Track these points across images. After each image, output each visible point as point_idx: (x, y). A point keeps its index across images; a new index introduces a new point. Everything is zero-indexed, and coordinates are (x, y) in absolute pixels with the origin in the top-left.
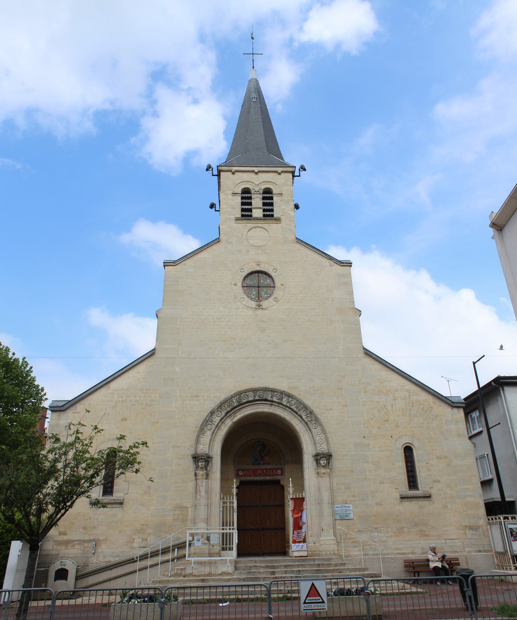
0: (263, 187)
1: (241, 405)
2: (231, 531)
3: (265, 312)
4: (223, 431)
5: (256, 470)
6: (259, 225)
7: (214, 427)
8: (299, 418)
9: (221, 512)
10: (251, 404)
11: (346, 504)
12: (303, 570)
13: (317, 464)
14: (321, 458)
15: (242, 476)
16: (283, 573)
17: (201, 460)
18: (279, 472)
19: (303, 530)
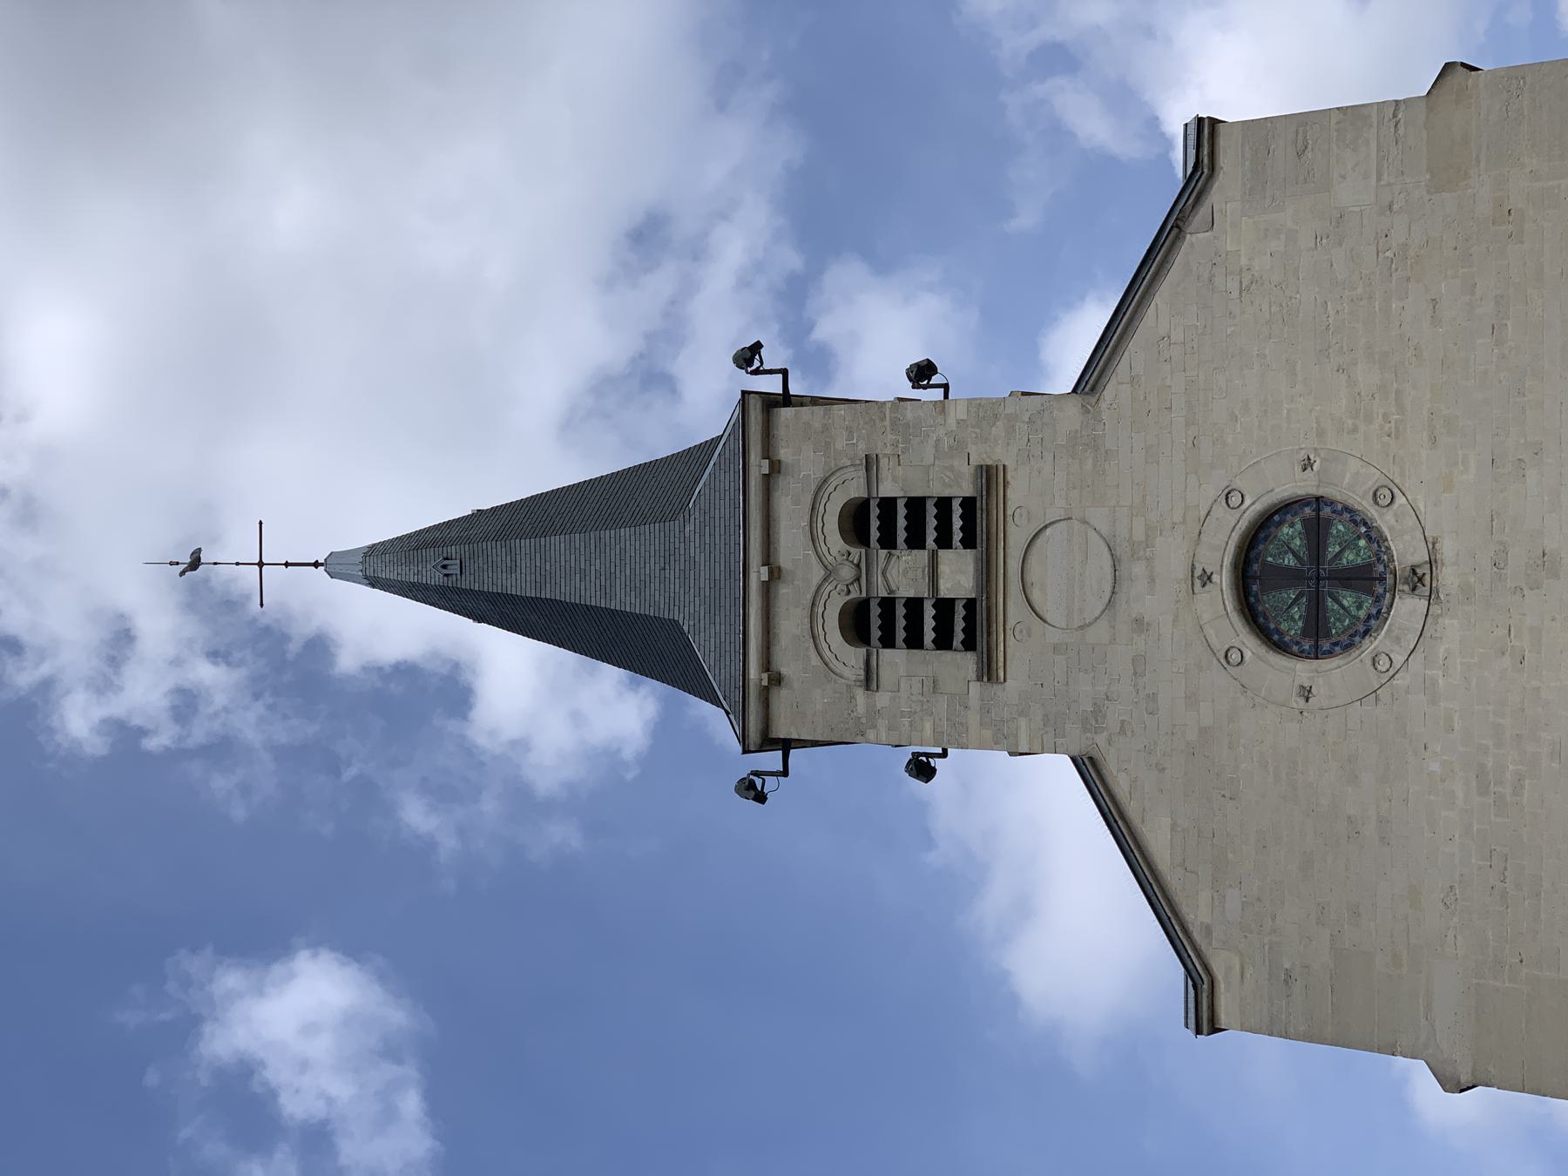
0: (835, 542)
3: (1447, 549)
6: (1014, 565)
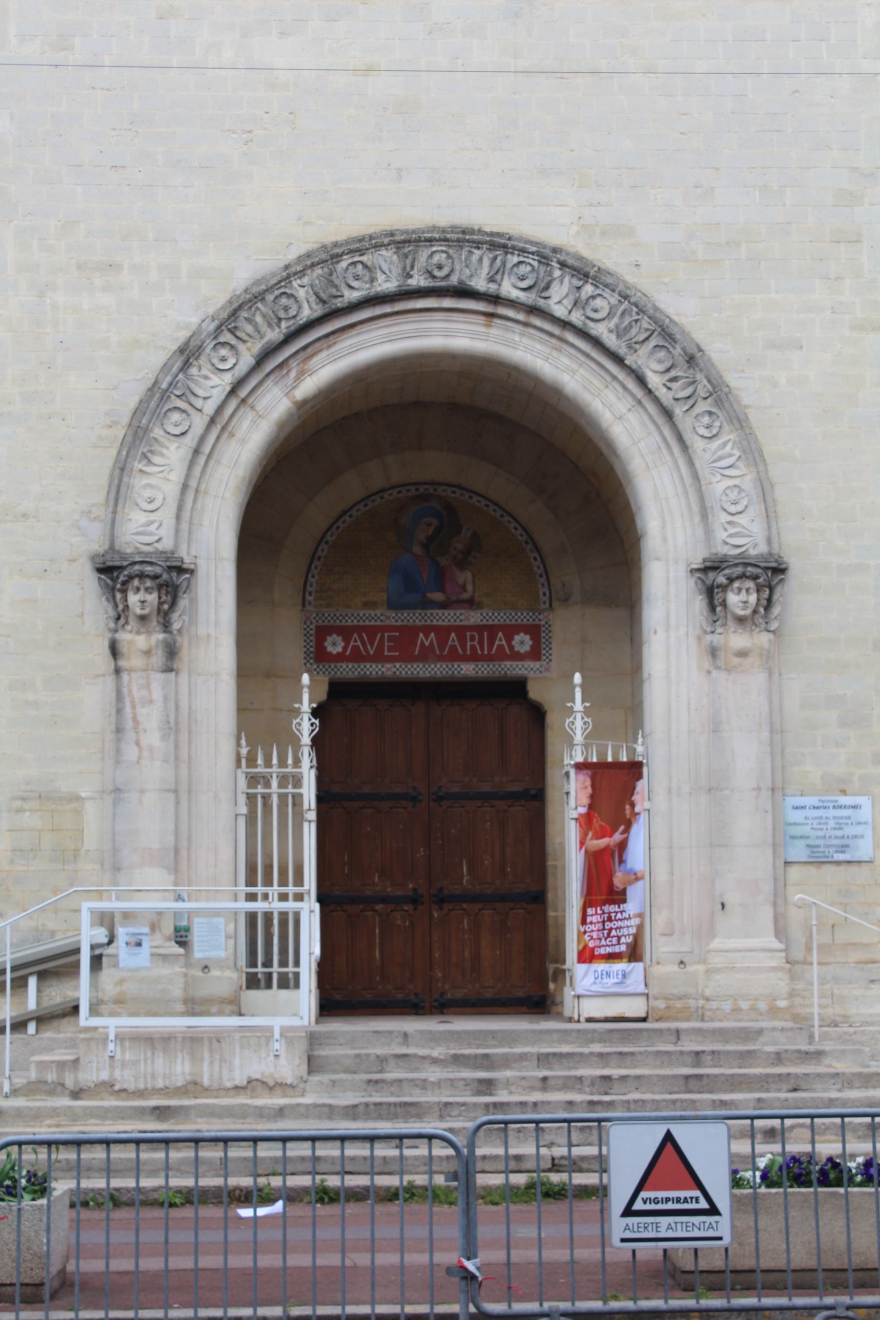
1: (336, 315)
2: (290, 905)
4: (243, 441)
5: (410, 632)
7: (199, 423)
8: (631, 384)
9: (242, 822)
10: (387, 309)
11: (844, 792)
12: (623, 1078)
13: (712, 608)
14: (731, 580)
15: (340, 658)
16: (533, 1089)
17: (139, 584)
18: (522, 642)
19: (631, 907)
